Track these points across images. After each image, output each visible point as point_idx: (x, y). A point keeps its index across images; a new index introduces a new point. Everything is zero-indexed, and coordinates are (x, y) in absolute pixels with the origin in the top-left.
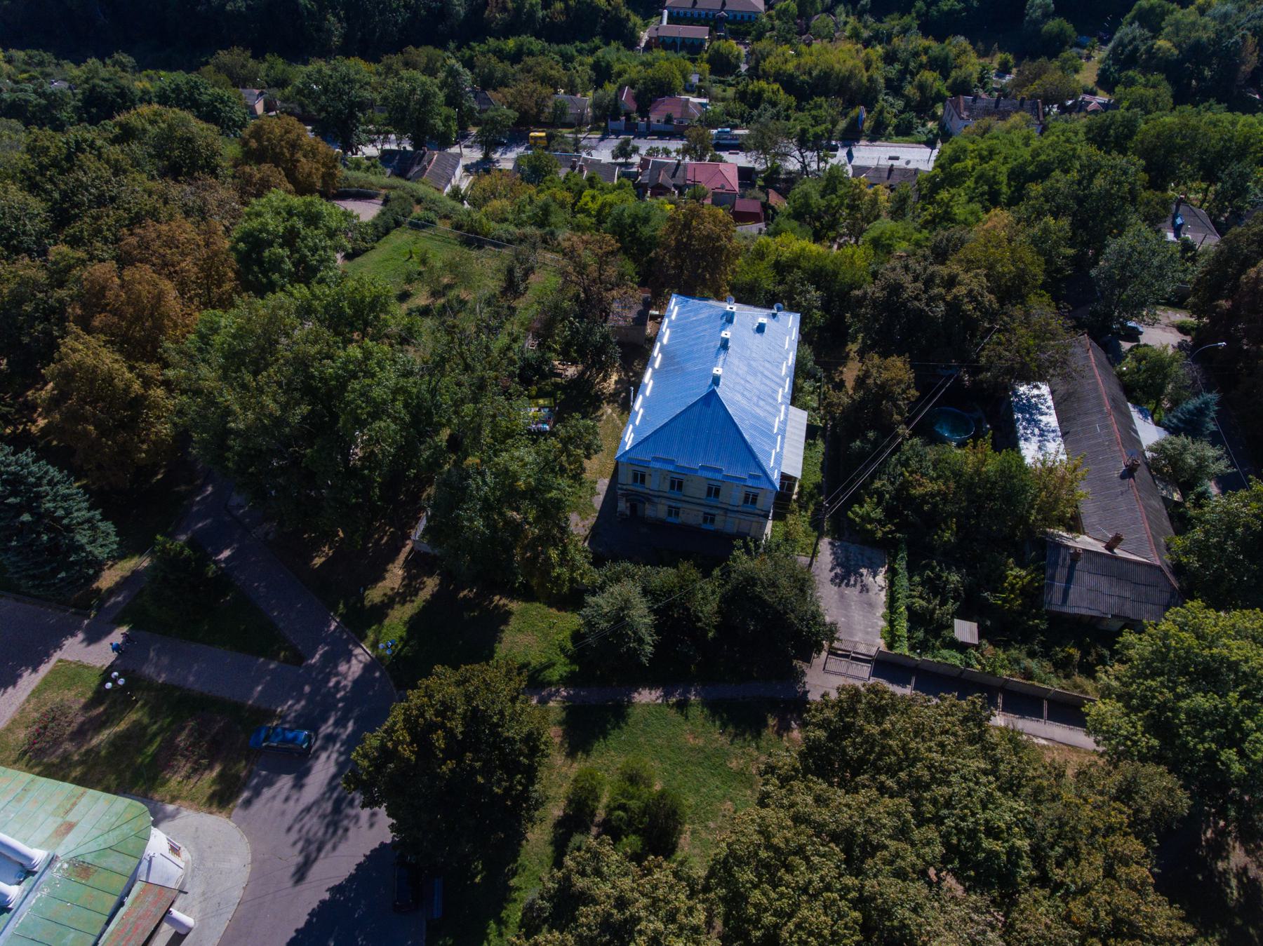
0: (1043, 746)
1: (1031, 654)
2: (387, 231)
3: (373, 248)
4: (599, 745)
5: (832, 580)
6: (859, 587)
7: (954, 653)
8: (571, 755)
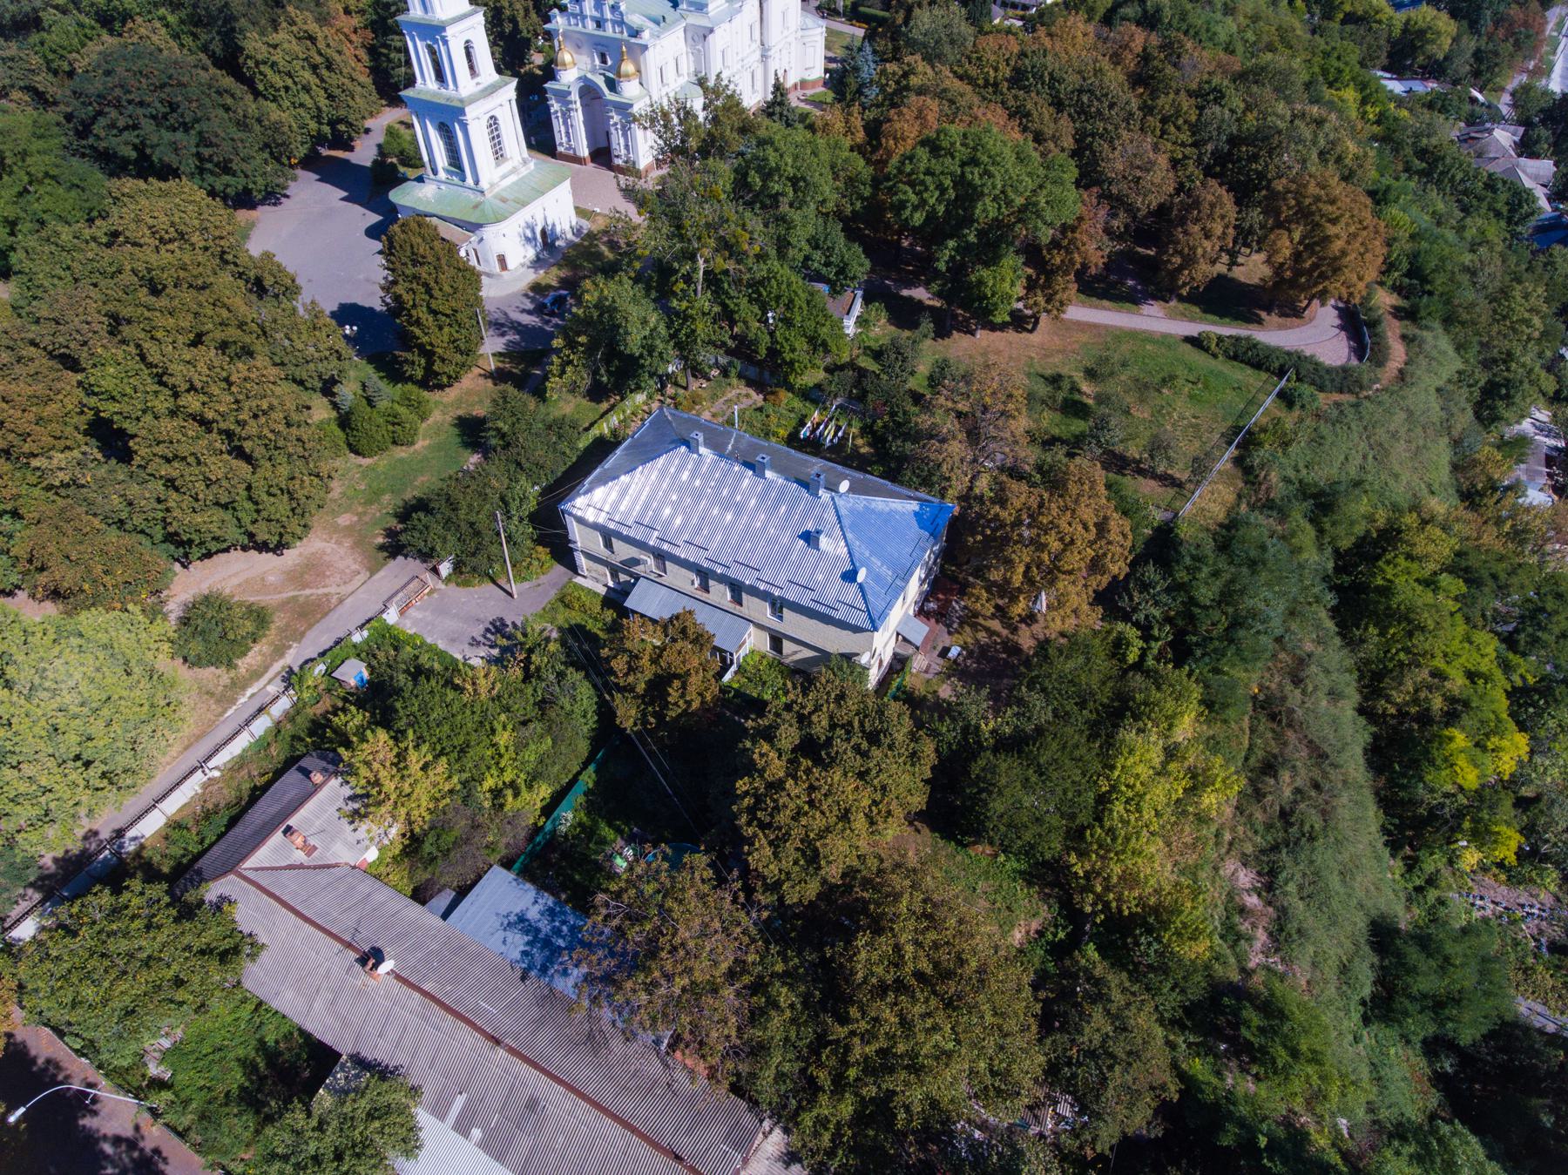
0: (225, 711)
1: (293, 737)
3: (1215, 356)
4: (456, 431)
5: (501, 620)
7: (344, 655)
8: (460, 418)
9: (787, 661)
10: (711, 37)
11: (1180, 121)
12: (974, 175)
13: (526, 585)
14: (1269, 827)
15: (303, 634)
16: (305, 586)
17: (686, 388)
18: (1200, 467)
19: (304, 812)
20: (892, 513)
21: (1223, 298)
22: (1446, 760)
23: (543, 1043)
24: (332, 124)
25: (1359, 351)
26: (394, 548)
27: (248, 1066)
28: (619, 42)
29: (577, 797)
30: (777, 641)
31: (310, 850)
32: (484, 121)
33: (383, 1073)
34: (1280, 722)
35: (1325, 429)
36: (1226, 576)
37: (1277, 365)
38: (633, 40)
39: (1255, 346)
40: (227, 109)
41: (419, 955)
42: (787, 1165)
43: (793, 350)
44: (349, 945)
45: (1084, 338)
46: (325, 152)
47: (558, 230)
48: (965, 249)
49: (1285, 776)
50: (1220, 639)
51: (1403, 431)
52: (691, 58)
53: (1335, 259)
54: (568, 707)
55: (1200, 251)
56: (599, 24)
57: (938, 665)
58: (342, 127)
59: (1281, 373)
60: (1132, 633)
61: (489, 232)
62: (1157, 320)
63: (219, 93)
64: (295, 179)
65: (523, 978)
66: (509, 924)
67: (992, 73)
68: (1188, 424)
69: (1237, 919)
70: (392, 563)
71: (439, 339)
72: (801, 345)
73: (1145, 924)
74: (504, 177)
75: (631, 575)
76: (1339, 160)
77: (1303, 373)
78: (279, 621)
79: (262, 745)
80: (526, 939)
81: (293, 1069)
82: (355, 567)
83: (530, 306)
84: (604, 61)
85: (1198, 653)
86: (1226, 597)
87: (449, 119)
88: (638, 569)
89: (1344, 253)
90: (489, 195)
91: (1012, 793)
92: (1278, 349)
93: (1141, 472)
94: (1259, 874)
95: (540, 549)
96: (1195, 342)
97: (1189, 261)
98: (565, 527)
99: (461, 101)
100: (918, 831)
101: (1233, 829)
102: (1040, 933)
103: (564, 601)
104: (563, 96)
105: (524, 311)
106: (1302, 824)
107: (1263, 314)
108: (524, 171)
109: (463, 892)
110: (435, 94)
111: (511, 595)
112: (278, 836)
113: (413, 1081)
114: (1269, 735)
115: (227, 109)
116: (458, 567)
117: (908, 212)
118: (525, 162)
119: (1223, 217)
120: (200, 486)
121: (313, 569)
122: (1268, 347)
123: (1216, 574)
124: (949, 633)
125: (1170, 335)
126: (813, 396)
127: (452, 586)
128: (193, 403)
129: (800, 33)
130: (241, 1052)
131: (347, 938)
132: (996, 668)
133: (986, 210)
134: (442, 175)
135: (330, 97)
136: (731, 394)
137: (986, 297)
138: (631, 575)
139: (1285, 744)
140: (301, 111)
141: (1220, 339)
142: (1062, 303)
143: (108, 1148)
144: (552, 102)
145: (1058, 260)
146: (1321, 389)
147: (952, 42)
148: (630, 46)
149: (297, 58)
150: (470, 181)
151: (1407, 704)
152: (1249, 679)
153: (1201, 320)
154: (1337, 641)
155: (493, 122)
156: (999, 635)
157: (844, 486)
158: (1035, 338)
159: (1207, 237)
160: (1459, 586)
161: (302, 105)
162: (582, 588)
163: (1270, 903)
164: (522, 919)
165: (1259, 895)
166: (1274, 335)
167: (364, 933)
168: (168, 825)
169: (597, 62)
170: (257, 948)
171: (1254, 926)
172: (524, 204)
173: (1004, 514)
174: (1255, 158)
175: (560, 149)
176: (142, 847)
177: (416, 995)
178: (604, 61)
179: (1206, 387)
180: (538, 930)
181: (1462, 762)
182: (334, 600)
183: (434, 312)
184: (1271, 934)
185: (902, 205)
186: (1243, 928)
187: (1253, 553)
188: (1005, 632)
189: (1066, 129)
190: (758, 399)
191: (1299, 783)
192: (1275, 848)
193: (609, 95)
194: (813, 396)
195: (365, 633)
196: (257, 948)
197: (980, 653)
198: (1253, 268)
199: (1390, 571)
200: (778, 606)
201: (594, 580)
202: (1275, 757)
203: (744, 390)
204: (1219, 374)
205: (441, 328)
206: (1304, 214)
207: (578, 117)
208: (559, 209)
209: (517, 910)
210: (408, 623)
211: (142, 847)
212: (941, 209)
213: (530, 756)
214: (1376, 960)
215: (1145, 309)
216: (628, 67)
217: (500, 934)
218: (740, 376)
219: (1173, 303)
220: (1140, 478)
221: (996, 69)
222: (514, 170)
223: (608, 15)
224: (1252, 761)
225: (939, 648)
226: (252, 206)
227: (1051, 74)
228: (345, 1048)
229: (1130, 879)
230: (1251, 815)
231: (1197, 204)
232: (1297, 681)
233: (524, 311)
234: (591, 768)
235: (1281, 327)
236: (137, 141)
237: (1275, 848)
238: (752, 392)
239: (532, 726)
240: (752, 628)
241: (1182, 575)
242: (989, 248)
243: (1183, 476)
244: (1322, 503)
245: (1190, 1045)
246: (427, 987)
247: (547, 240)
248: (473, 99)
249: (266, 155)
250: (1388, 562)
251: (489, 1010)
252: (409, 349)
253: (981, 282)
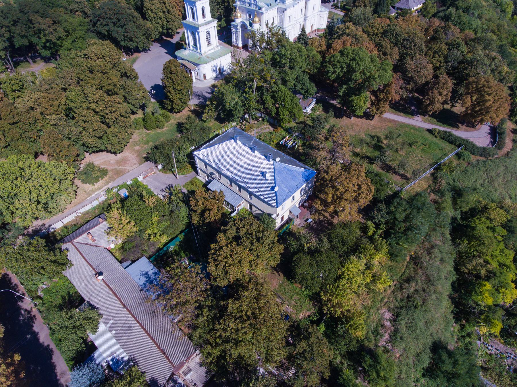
0: (88, 197)
2: (451, 142)
3: (436, 137)
5: (172, 185)
6: (164, 189)
9: (254, 213)
10: (285, 12)
11: (440, 53)
12: (353, 64)
13: (182, 176)
14: (402, 300)
15: (115, 179)
16: (120, 165)
17: (249, 123)
18: (416, 174)
19: (94, 229)
21: (446, 117)
22: (481, 292)
23: (138, 311)
24: (167, 29)
25: (493, 143)
26: (147, 159)
27: (63, 298)
28: (254, 11)
29: (177, 242)
30: (251, 206)
31: (94, 240)
32: (205, 32)
33: (92, 307)
34: (417, 265)
35: (469, 168)
36: (408, 212)
37: (458, 143)
38: (259, 11)
39: (451, 135)
40: (134, 22)
41: (113, 277)
42: (201, 366)
43: (284, 115)
44: (94, 269)
45: (390, 125)
46: (165, 38)
47: (225, 68)
48: (349, 89)
49: (413, 284)
50: (402, 233)
51: (502, 174)
52: (279, 18)
53: (488, 108)
54: (178, 214)
55: (436, 99)
56: (250, 5)
57: (304, 224)
58: (170, 31)
59: (459, 146)
60: (370, 224)
61: (201, 67)
62: (419, 122)
63: (133, 17)
64: (152, 45)
65: (141, 290)
66: (143, 274)
67: (376, 31)
68: (416, 160)
69: (380, 328)
70: (146, 163)
71: (175, 97)
72: (287, 113)
73: (342, 321)
74: (210, 50)
75: (212, 177)
76: (499, 73)
77: (467, 147)
78: (110, 174)
79: (94, 209)
80: (146, 279)
81: (73, 301)
82: (135, 162)
83: (210, 91)
84: (250, 17)
85: (393, 236)
86: (407, 218)
87: (194, 30)
88: (213, 176)
89: (491, 106)
90: (203, 55)
91: (304, 267)
92: (460, 138)
93: (395, 173)
94: (393, 315)
95: (189, 165)
96: (430, 131)
97: (432, 103)
98: (194, 160)
99: (198, 25)
100: (279, 275)
101: (389, 298)
102: (309, 316)
103: (191, 183)
104: (236, 27)
105: (207, 93)
106: (414, 302)
107: (460, 125)
108: (216, 49)
109: (133, 262)
110: (192, 23)
111: (176, 177)
112: (85, 234)
113: (101, 312)
114: (412, 269)
115: (134, 22)
116: (164, 168)
117: (330, 74)
118: (217, 46)
119: (447, 88)
120: (91, 130)
121: (124, 161)
122: (456, 136)
123: (405, 210)
124: (311, 214)
125: (422, 128)
126: (289, 131)
127: (161, 172)
128: (93, 106)
129: (319, 13)
130: (63, 294)
131: (94, 267)
132: (319, 228)
133: (358, 76)
134: (191, 48)
135: (167, 21)
136: (263, 127)
137: (353, 106)
138: (212, 177)
139: (417, 274)
140: (158, 25)
141: (439, 131)
142: (382, 112)
143: (23, 312)
144: (233, 28)
145: (382, 96)
146: (473, 154)
147: (365, 20)
148: (258, 13)
149: (159, 9)
150: (199, 50)
151: (472, 270)
152: (409, 249)
153: (435, 124)
154: (450, 243)
155: (208, 33)
156: (327, 218)
157: (278, 159)
158: (372, 122)
159: (440, 95)
160: (504, 232)
161: (158, 23)
162: (198, 180)
163: (393, 326)
164: (147, 273)
165: (391, 322)
166: (461, 133)
167: (100, 267)
168: (63, 227)
169: (248, 17)
170: (72, 265)
171: (385, 332)
172: (214, 59)
173: (327, 177)
174: (466, 69)
175: (233, 44)
176: (55, 231)
177: (107, 288)
178: (250, 17)
179: (429, 147)
180: (150, 278)
181: (486, 294)
182: (127, 171)
183: (174, 89)
184: (390, 336)
185: (328, 72)
186: (380, 331)
187: (419, 205)
188: (329, 217)
189: (396, 53)
190: (271, 129)
191: (417, 288)
192: (401, 308)
193: (249, 28)
194: (289, 131)
195: (132, 182)
196: (72, 265)
197: (319, 223)
198: (458, 109)
199: (477, 221)
200: (251, 194)
201: (202, 178)
202: (412, 277)
203: (268, 126)
204: (435, 144)
205: (176, 94)
206: (478, 91)
207: (240, 34)
208: (226, 62)
209: (146, 271)
210: (145, 181)
211: (55, 231)
212: (341, 74)
213: (162, 226)
214: (431, 355)
215: (416, 118)
216: (257, 19)
217: (139, 276)
218: (268, 121)
219: (427, 117)
220: (394, 175)
221: (378, 30)
222: (213, 49)
223: (253, 2)
224: (403, 277)
225: (306, 219)
226: (139, 52)
227: (396, 33)
228: (86, 299)
229: (339, 305)
230: (397, 295)
231: (438, 83)
232: (429, 253)
233: (207, 93)
234: (183, 234)
235: (465, 130)
236: (108, 29)
237: (401, 308)
238: (270, 127)
239: (165, 217)
240: (244, 201)
241: (392, 209)
242: (358, 91)
243: (409, 175)
244: (458, 194)
245: (348, 365)
246: (111, 286)
247: (221, 72)
248: (202, 25)
249: (144, 37)
250: (478, 218)
251: (127, 298)
252: (166, 99)
253: (353, 101)
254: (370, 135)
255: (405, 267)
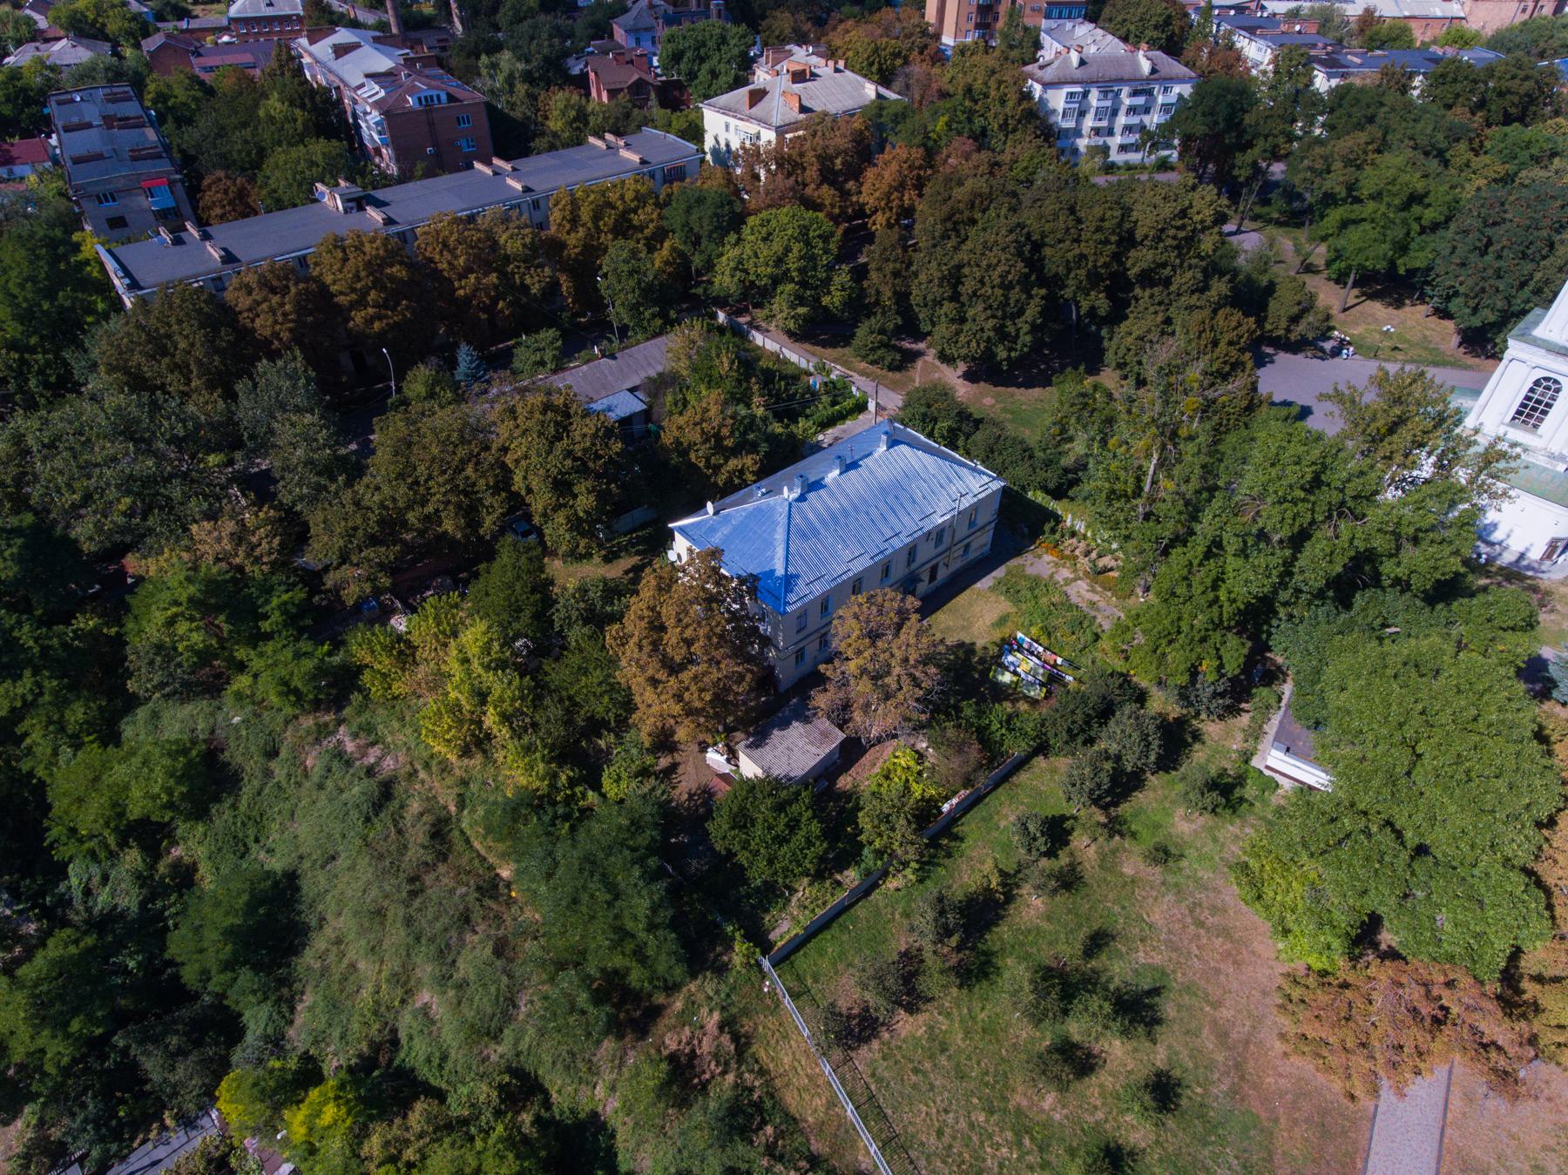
20: (770, 544)
254: (1156, 991)
255: (483, 852)
